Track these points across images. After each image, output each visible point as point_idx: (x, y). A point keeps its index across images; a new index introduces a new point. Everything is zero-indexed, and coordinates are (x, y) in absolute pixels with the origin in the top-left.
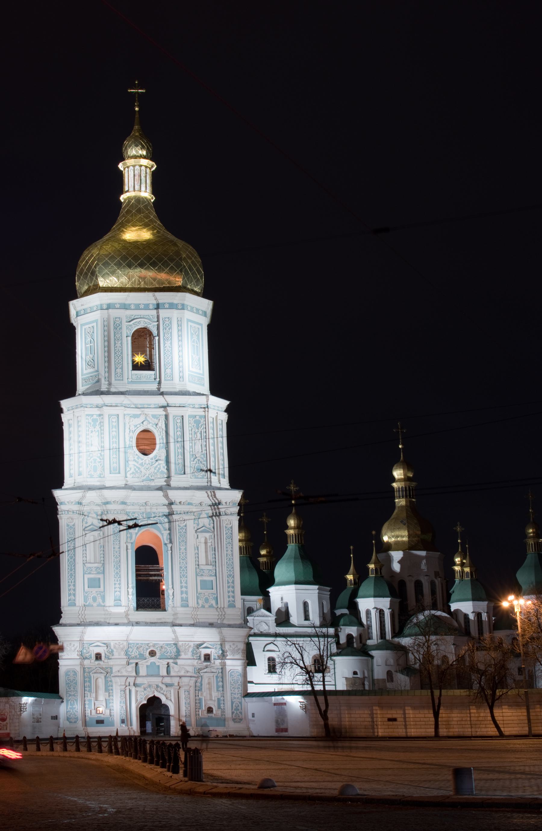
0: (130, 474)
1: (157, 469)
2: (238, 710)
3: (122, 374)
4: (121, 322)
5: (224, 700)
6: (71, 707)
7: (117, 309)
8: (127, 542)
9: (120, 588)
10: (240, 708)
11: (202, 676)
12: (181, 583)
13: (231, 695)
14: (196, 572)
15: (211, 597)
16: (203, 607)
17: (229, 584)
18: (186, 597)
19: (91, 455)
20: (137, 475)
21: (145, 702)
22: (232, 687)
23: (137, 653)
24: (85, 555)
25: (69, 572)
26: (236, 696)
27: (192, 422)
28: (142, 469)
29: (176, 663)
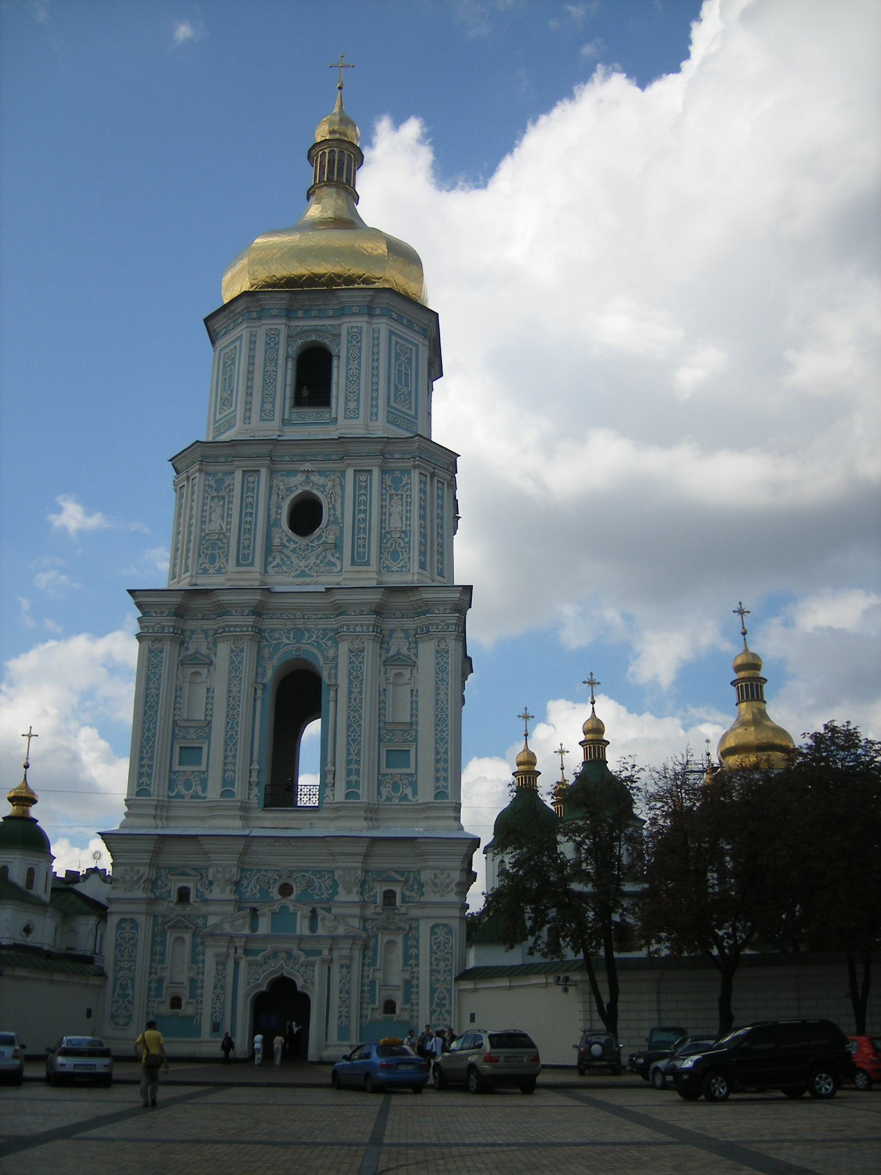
0: (273, 567)
1: (321, 557)
3: (273, 411)
4: (278, 335)
5: (417, 986)
6: (120, 992)
7: (274, 316)
8: (256, 682)
9: (234, 764)
10: (447, 1002)
11: (376, 936)
12: (349, 754)
13: (431, 975)
14: (379, 734)
15: (404, 782)
16: (389, 799)
17: (439, 757)
18: (356, 781)
19: (207, 538)
20: (285, 569)
21: (264, 988)
22: (436, 956)
23: (255, 887)
24: (178, 706)
25: (143, 734)
26: (441, 977)
27: (388, 482)
28: (293, 559)
29: (329, 910)
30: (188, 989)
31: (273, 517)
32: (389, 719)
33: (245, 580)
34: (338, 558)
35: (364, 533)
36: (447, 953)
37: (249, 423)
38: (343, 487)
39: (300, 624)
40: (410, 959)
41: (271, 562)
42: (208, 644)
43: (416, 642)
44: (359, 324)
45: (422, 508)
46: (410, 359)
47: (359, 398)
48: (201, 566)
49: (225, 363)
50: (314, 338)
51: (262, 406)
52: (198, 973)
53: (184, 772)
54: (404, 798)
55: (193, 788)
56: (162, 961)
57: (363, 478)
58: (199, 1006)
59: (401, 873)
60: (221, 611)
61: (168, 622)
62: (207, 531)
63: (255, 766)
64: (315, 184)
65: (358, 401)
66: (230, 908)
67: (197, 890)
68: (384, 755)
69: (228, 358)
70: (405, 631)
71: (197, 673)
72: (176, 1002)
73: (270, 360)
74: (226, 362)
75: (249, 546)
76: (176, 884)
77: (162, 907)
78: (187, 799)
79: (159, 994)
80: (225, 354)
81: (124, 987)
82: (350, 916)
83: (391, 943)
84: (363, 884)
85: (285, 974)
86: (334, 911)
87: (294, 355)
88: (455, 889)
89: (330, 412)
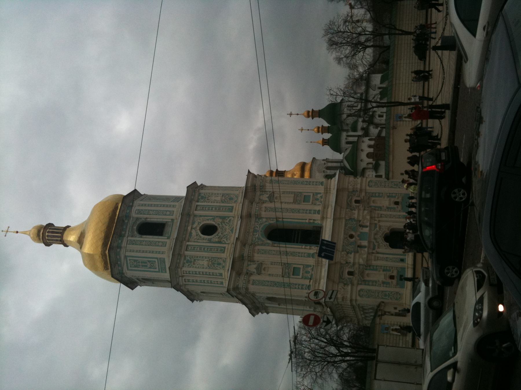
0: (227, 241)
1: (227, 224)
2: (397, 184)
5: (390, 193)
7: (122, 241)
8: (272, 246)
9: (302, 253)
10: (396, 183)
11: (371, 206)
12: (303, 213)
16: (321, 202)
19: (210, 266)
20: (229, 237)
27: (202, 200)
28: (225, 234)
29: (360, 221)
30: (387, 272)
31: (207, 241)
32: (292, 201)
33: (230, 250)
34: (228, 218)
35: (221, 208)
36: (379, 182)
37: (165, 252)
38: (201, 216)
39: (252, 230)
40: (380, 195)
41: (225, 242)
42: (253, 264)
43: (265, 191)
44: (135, 210)
47: (165, 211)
48: (220, 268)
49: (135, 267)
50: (135, 228)
51: (160, 246)
52: (381, 268)
53: (302, 274)
54: (321, 197)
55: (309, 270)
56: (376, 282)
57: (199, 208)
58: (394, 268)
60: (242, 258)
61: (242, 277)
62: (207, 266)
63: (304, 247)
64: (61, 241)
65: (166, 211)
66: (357, 255)
67: (349, 268)
68: (305, 203)
69: (133, 264)
70: (260, 195)
71: (264, 269)
72: (392, 277)
73: (141, 243)
74: (135, 266)
75: (218, 249)
76: (346, 276)
77: (355, 282)
78: (313, 272)
79: (389, 283)
80: (131, 267)
81: (386, 295)
82: (363, 213)
83: (374, 202)
84: (352, 210)
85: (383, 236)
86: (361, 219)
87: (141, 235)
88: (356, 179)
89: (168, 222)
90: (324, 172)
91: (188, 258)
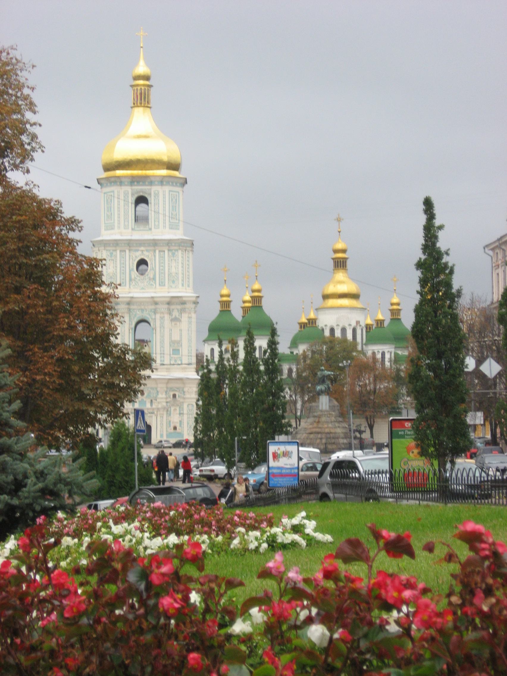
27: (170, 254)
31: (131, 267)
32: (173, 339)
38: (155, 256)
39: (143, 307)
45: (183, 264)
46: (176, 200)
49: (107, 201)
50: (141, 194)
57: (162, 253)
59: (178, 388)
65: (159, 222)
68: (171, 350)
83: (175, 410)
84: (166, 393)
86: (158, 400)
90: (338, 325)
91: (114, 253)
